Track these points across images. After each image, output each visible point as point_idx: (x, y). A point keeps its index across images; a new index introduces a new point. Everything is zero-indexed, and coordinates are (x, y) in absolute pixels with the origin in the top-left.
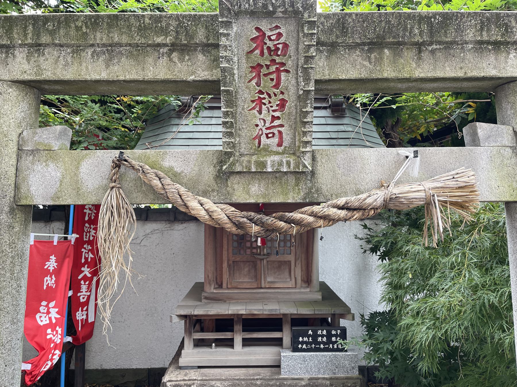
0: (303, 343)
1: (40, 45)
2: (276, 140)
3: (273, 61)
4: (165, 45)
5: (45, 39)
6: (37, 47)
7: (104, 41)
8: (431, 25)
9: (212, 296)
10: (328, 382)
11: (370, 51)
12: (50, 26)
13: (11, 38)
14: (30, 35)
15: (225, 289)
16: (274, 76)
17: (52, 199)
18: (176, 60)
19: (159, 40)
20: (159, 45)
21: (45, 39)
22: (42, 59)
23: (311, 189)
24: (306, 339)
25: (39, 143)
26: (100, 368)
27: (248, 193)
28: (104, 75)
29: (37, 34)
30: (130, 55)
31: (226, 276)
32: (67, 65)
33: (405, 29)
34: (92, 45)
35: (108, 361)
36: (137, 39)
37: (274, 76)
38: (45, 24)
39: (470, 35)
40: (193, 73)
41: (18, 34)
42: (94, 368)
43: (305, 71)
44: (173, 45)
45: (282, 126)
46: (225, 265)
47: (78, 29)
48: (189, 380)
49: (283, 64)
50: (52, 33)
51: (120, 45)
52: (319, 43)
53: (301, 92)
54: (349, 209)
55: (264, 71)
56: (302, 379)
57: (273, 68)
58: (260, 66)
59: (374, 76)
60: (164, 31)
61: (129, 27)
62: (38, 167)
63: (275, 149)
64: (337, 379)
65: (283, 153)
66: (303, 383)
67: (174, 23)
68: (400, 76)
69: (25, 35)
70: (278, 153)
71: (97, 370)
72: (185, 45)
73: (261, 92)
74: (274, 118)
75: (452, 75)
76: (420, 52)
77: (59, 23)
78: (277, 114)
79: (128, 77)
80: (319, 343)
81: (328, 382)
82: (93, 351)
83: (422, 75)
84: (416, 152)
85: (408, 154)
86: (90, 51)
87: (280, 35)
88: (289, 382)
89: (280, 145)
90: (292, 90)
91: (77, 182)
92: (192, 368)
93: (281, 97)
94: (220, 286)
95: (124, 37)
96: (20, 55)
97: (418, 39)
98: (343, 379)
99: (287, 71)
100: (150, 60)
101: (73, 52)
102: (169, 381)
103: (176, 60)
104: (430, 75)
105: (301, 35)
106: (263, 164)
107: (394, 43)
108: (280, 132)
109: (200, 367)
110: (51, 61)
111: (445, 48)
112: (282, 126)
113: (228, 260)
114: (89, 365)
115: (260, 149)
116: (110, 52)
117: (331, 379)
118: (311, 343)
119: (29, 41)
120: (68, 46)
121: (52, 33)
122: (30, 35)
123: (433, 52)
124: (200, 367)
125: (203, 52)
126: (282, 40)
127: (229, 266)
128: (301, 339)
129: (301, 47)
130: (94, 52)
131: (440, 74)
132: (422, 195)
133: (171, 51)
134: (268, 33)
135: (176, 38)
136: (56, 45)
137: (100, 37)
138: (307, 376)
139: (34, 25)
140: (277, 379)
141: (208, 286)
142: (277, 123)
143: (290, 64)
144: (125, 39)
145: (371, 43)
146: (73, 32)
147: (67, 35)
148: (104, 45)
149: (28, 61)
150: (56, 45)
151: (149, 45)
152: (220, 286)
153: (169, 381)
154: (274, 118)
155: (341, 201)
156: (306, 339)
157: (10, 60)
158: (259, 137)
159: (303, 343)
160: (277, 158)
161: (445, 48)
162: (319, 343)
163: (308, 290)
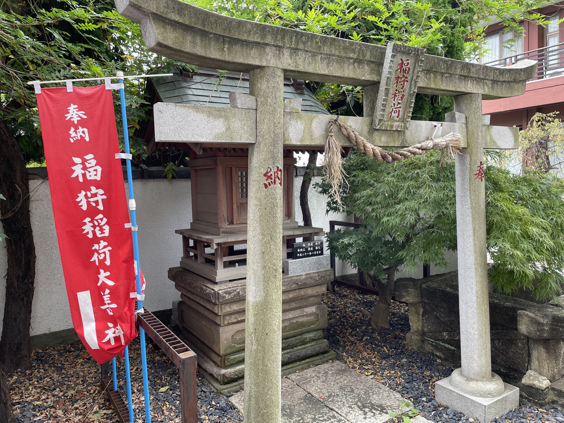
0: (300, 253)
1: (297, 49)
2: (397, 114)
3: (404, 75)
4: (353, 58)
5: (301, 46)
6: (295, 51)
7: (328, 52)
8: (447, 64)
9: (227, 230)
10: (317, 275)
11: (427, 74)
12: (304, 39)
13: (284, 42)
14: (293, 43)
15: (236, 225)
16: (402, 83)
17: (300, 141)
18: (356, 67)
19: (351, 55)
20: (350, 58)
21: (301, 46)
22: (297, 58)
23: (403, 139)
24: (301, 250)
25: (293, 108)
26: (48, 332)
27: (381, 141)
28: (326, 72)
29: (297, 43)
30: (337, 62)
31: (235, 215)
32: (309, 63)
33: (439, 66)
34: (322, 53)
35: (57, 323)
36: (343, 54)
37: (402, 83)
38: (301, 37)
39: (458, 72)
40: (364, 76)
41: (288, 40)
42: (42, 333)
43: (416, 82)
44: (356, 59)
45: (400, 107)
46: (235, 206)
47: (317, 43)
48: (233, 287)
49: (406, 78)
50: (305, 43)
51: (334, 55)
52: (423, 70)
53: (412, 92)
54: (422, 150)
55: (400, 80)
56: (302, 275)
57: (403, 79)
58: (399, 77)
59: (428, 86)
60: (353, 51)
61: (339, 46)
62: (293, 122)
63: (396, 119)
64: (320, 272)
65: (398, 121)
66: (304, 277)
67: (358, 47)
68: (436, 88)
69: (291, 42)
70: (397, 121)
71: (45, 335)
72: (361, 60)
73: (396, 90)
74: (399, 103)
75: (451, 89)
76: (442, 77)
77: (308, 38)
78: (400, 102)
79: (337, 74)
80: (309, 252)
81: (317, 275)
82: (39, 316)
83: (443, 88)
84: (442, 124)
85: (436, 124)
86: (319, 56)
87: (408, 63)
88: (296, 278)
89: (398, 117)
90: (407, 90)
91: (311, 132)
92: (226, 282)
93: (403, 93)
94: (231, 223)
95: (337, 51)
96: (286, 53)
97: (443, 71)
98: (323, 271)
99: (407, 81)
100: (346, 66)
101: (312, 56)
102: (220, 290)
103: (356, 67)
104: (446, 88)
105: (417, 65)
106: (392, 126)
107: (435, 71)
108: (399, 111)
109: (230, 281)
110: (302, 60)
111: (450, 76)
112: (400, 107)
113: (237, 202)
114: (35, 331)
115: (391, 118)
116: (329, 59)
117: (317, 272)
118: (304, 252)
119: (293, 46)
120: (310, 52)
121: (305, 43)
122: (293, 43)
123: (446, 77)
124: (230, 281)
125: (367, 64)
126: (408, 66)
127: (238, 207)
128: (299, 250)
129: (416, 71)
130: (321, 57)
131: (448, 89)
132: (445, 143)
133: (354, 62)
134: (405, 62)
135: (358, 56)
136: (305, 50)
137: (326, 50)
138: (304, 273)
139: (296, 36)
140: (288, 278)
141: (224, 223)
142: (399, 106)
143: (409, 78)
144: (337, 53)
145: (428, 70)
146: (314, 45)
147: (311, 45)
148: (327, 54)
149: (291, 58)
150: (305, 50)
151: (346, 58)
152: (231, 223)
153: (220, 290)
154: (399, 103)
155: (419, 145)
156: (301, 250)
157: (281, 55)
158: (391, 113)
159: (300, 253)
160: (397, 123)
161: (450, 76)
162: (309, 252)
163: (289, 221)
